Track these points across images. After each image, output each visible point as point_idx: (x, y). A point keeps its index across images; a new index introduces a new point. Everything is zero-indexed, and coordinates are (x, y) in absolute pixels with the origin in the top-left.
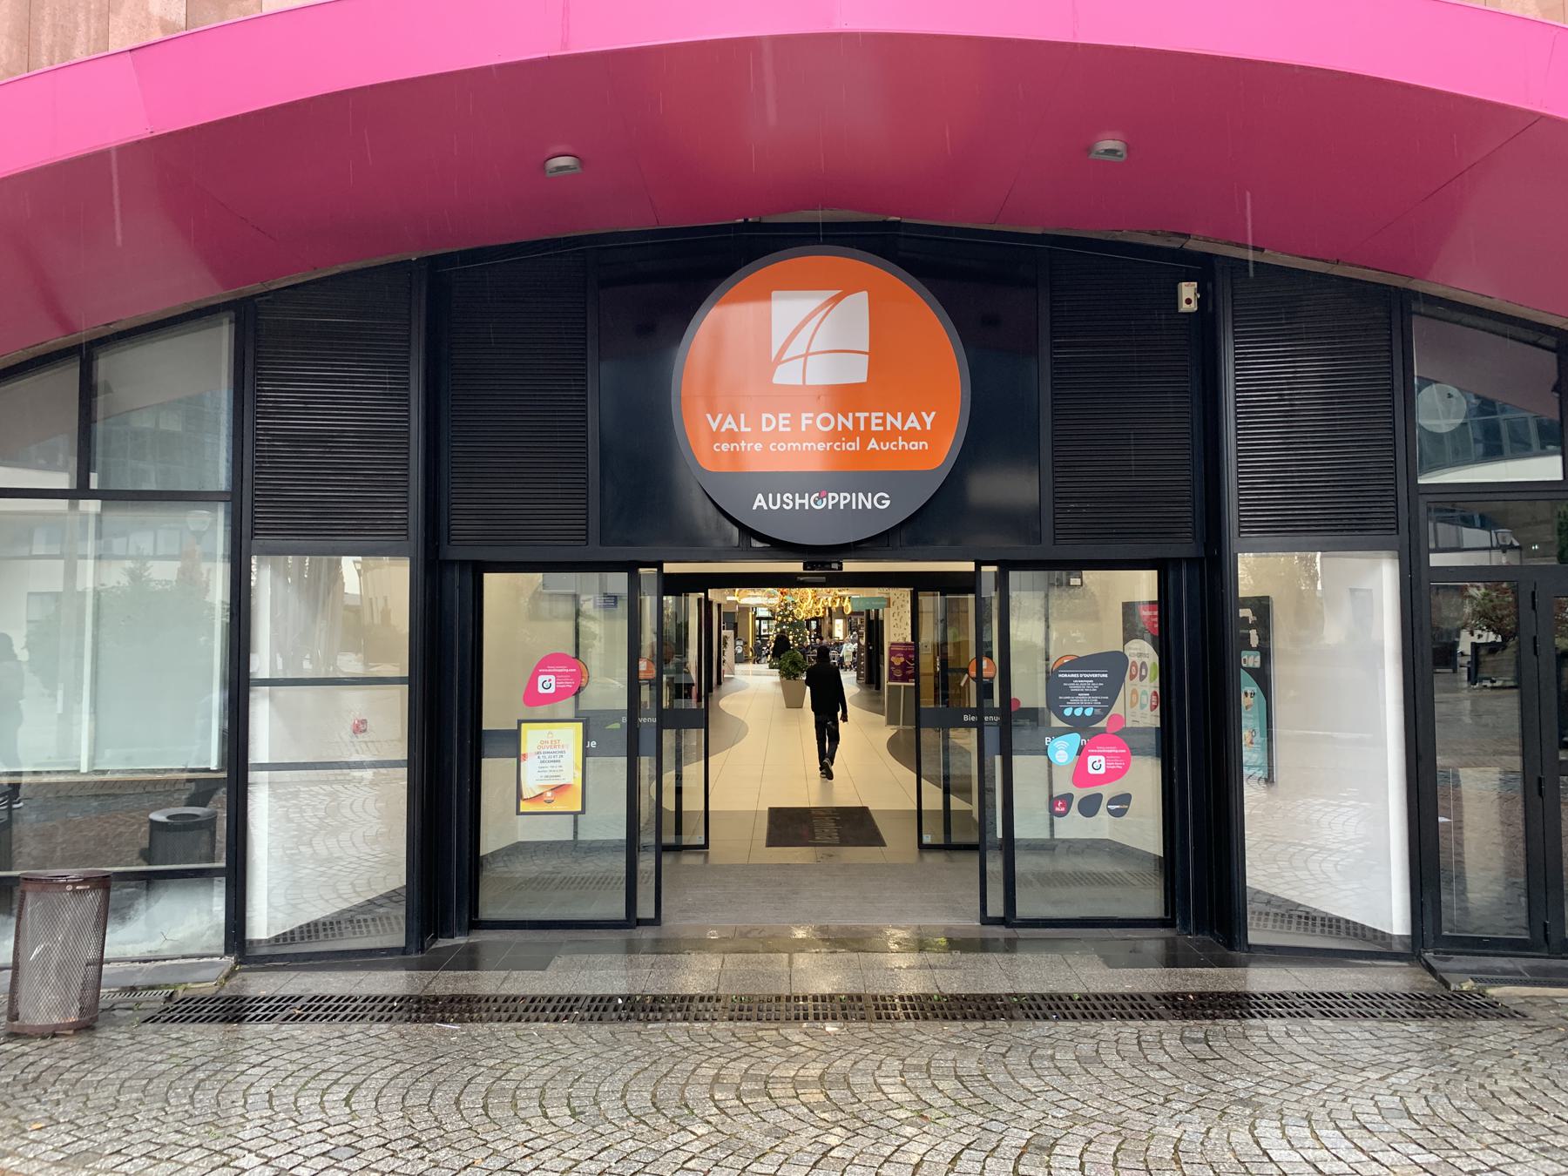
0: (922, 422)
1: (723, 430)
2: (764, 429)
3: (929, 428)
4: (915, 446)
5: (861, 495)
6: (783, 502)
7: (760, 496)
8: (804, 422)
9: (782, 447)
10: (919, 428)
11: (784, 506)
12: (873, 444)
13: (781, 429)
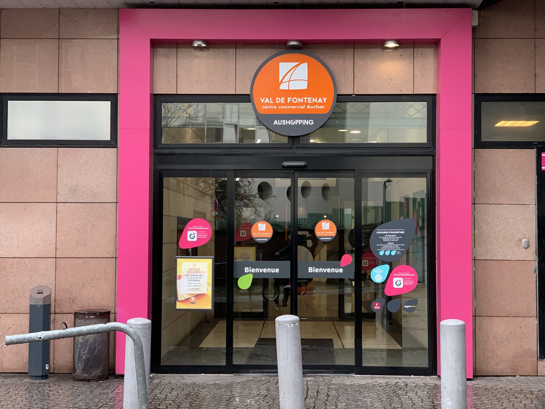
0: (323, 100)
1: (265, 102)
2: (277, 102)
3: (325, 102)
4: (321, 107)
5: (305, 120)
6: (282, 122)
7: (276, 121)
8: (289, 100)
9: (282, 107)
10: (322, 102)
11: (283, 124)
12: (309, 107)
13: (282, 102)
